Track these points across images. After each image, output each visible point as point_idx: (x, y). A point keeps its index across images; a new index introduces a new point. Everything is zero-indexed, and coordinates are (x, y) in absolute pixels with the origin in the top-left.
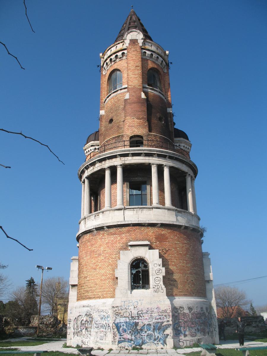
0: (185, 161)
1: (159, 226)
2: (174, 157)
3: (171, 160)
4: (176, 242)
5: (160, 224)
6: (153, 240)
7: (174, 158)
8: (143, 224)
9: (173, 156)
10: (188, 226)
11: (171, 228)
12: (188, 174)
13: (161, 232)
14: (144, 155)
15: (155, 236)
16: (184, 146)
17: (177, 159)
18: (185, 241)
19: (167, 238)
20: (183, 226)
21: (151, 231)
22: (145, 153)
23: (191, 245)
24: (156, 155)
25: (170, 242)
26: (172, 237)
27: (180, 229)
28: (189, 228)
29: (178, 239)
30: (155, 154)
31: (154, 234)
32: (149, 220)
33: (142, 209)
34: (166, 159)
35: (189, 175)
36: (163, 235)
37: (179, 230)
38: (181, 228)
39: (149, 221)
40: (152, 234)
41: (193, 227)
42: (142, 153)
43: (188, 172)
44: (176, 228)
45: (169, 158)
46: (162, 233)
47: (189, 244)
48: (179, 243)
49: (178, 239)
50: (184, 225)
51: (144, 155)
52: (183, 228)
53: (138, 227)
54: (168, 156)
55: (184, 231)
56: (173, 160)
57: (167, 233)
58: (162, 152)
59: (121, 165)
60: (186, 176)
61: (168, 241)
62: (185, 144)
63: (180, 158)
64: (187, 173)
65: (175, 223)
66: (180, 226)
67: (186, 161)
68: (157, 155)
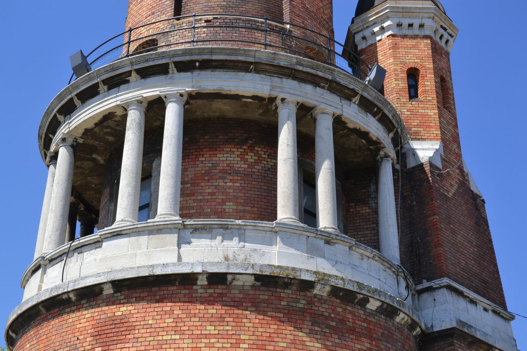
0: (251, 63)
1: (111, 291)
2: (196, 61)
3: (189, 74)
4: (164, 338)
5: (110, 285)
6: (84, 344)
7: (197, 64)
8: (65, 297)
9: (187, 58)
10: (223, 270)
11: (154, 289)
12: (278, 102)
13: (114, 310)
14: (106, 88)
15: (93, 331)
16: (399, 25)
17: (207, 65)
18: (209, 328)
19: (134, 328)
20: (200, 277)
21: (84, 319)
22: (105, 82)
23: (242, 337)
24: (134, 74)
25: (140, 340)
26: (150, 322)
27: (192, 289)
28: (229, 277)
29: (174, 324)
30: (129, 73)
31: (91, 323)
32: (75, 281)
33: (79, 250)
34: (170, 76)
35: (283, 100)
36: (122, 321)
37: (186, 292)
38: (196, 284)
39: (77, 283)
40: (88, 324)
41: (250, 271)
42: (96, 85)
43: (274, 94)
44: (174, 288)
45: (179, 70)
46: (117, 314)
47: (229, 337)
48: (178, 337)
49: (174, 324)
50: (198, 269)
51: (106, 88)
52: (206, 283)
53: (57, 309)
54: (172, 66)
55: (209, 291)
56: (196, 73)
57: (132, 312)
58: (147, 61)
59: (64, 140)
60: (277, 108)
61: (131, 336)
62: (403, 17)
63: (214, 57)
64: (272, 100)
65: (158, 271)
66: (188, 279)
67: (251, 60)
68: (138, 77)
